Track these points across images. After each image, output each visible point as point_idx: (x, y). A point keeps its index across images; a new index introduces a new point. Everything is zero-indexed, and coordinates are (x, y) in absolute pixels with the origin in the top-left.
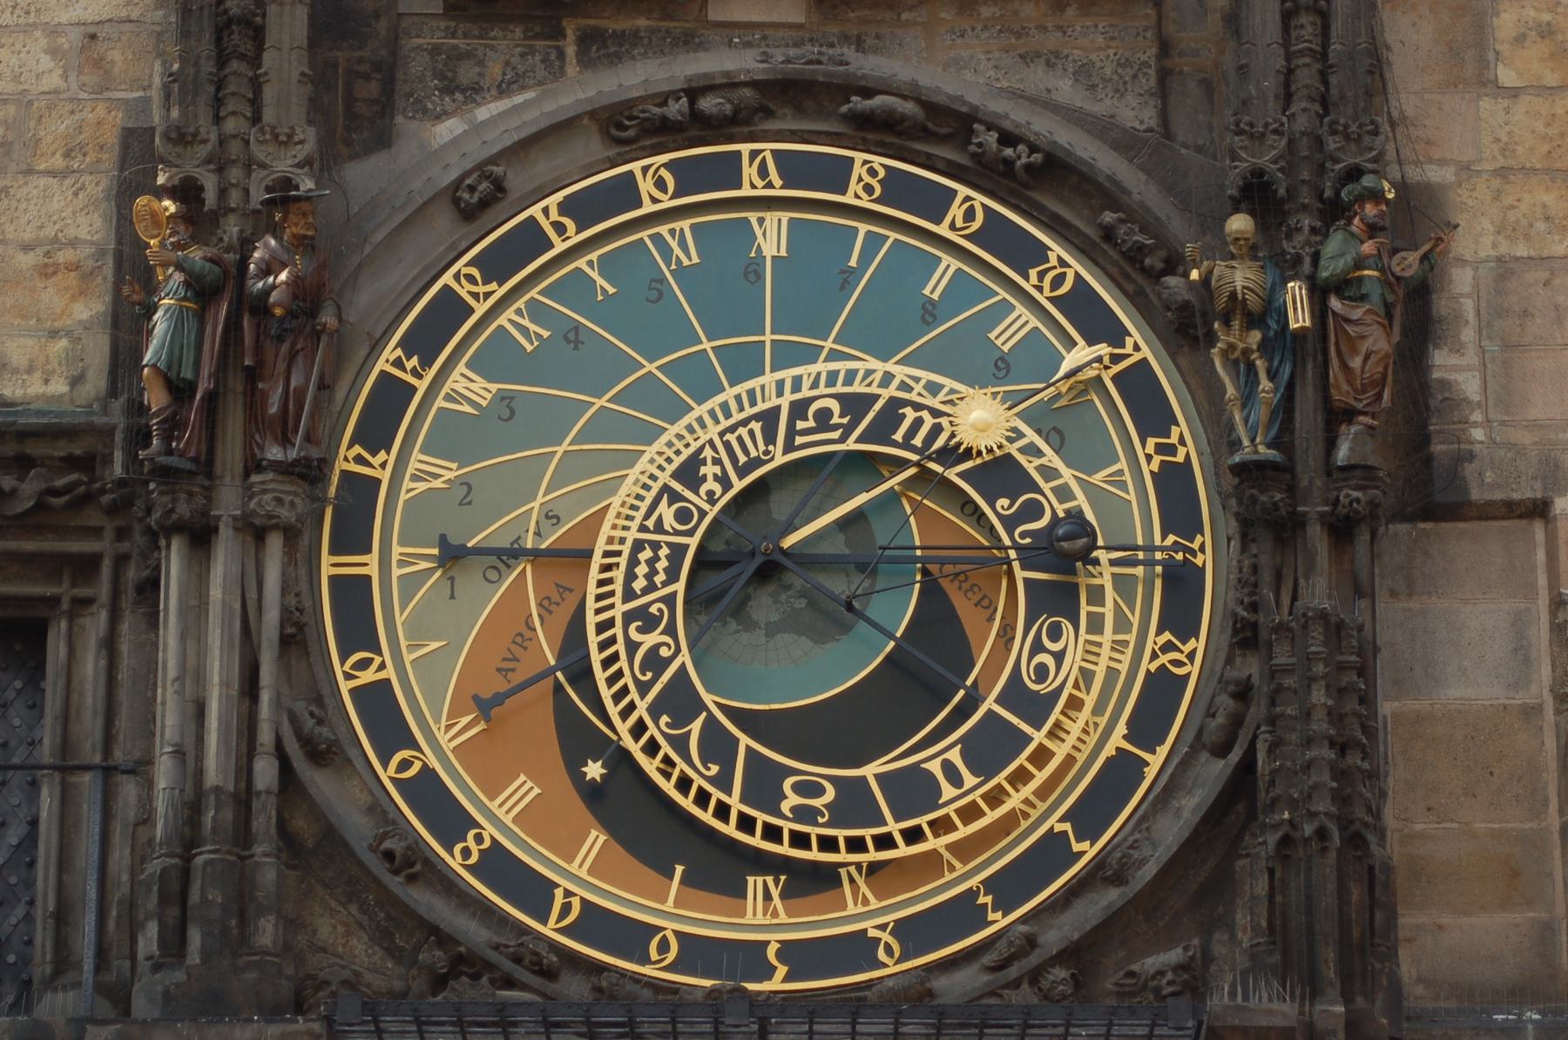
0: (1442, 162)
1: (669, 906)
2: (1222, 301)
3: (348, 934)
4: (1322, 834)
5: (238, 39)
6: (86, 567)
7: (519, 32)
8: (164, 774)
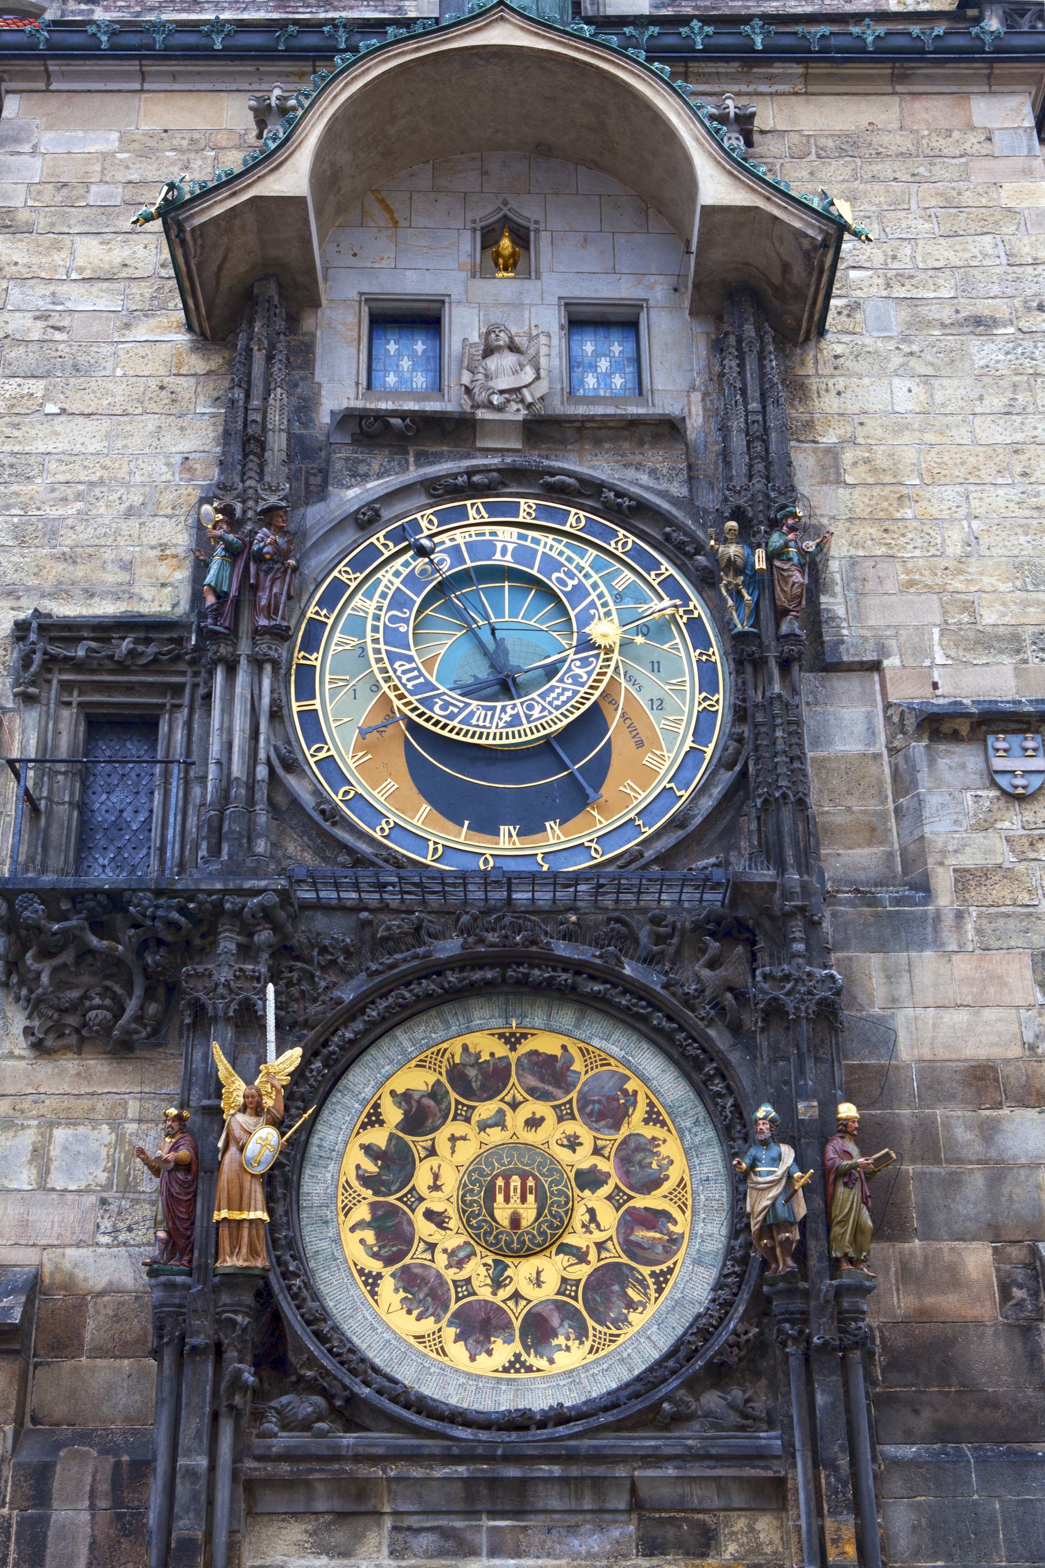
0: (822, 516)
1: (462, 839)
2: (723, 564)
3: (302, 851)
4: (784, 796)
5: (252, 446)
6: (177, 690)
7: (387, 452)
8: (212, 772)
